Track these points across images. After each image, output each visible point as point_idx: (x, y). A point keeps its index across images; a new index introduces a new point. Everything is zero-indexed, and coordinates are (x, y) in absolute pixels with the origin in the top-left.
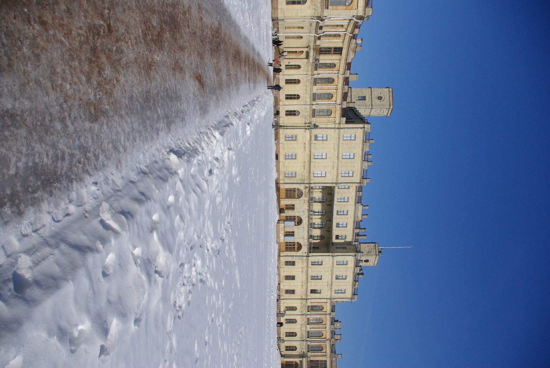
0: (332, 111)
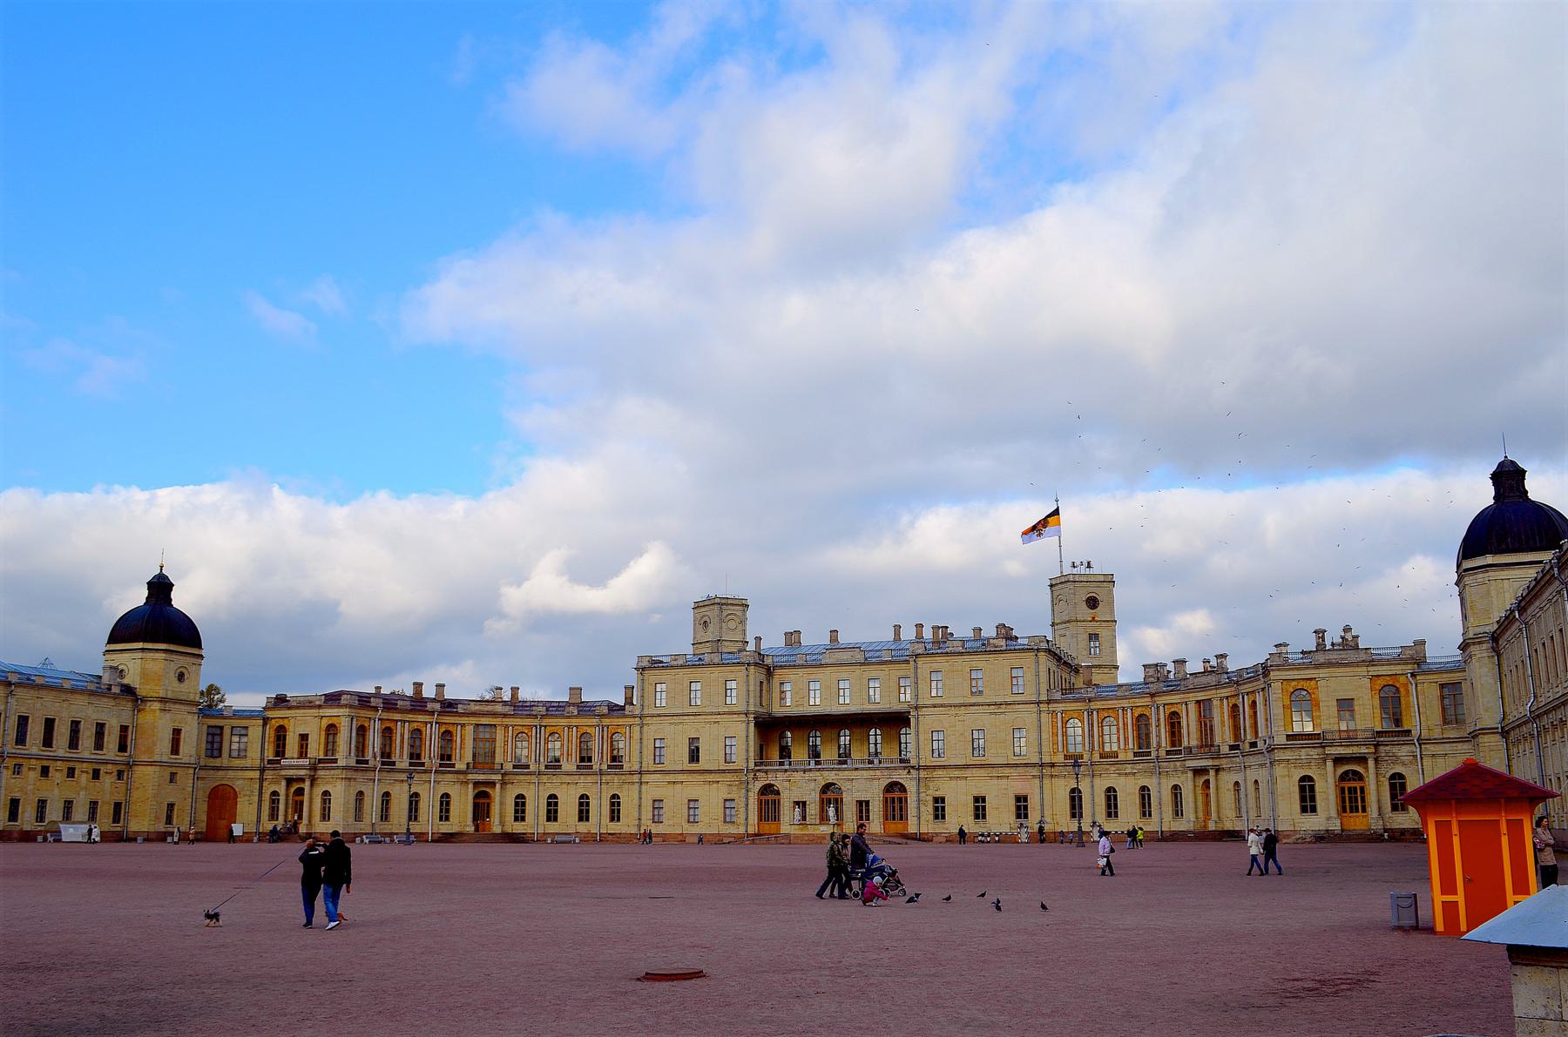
0: (613, 732)
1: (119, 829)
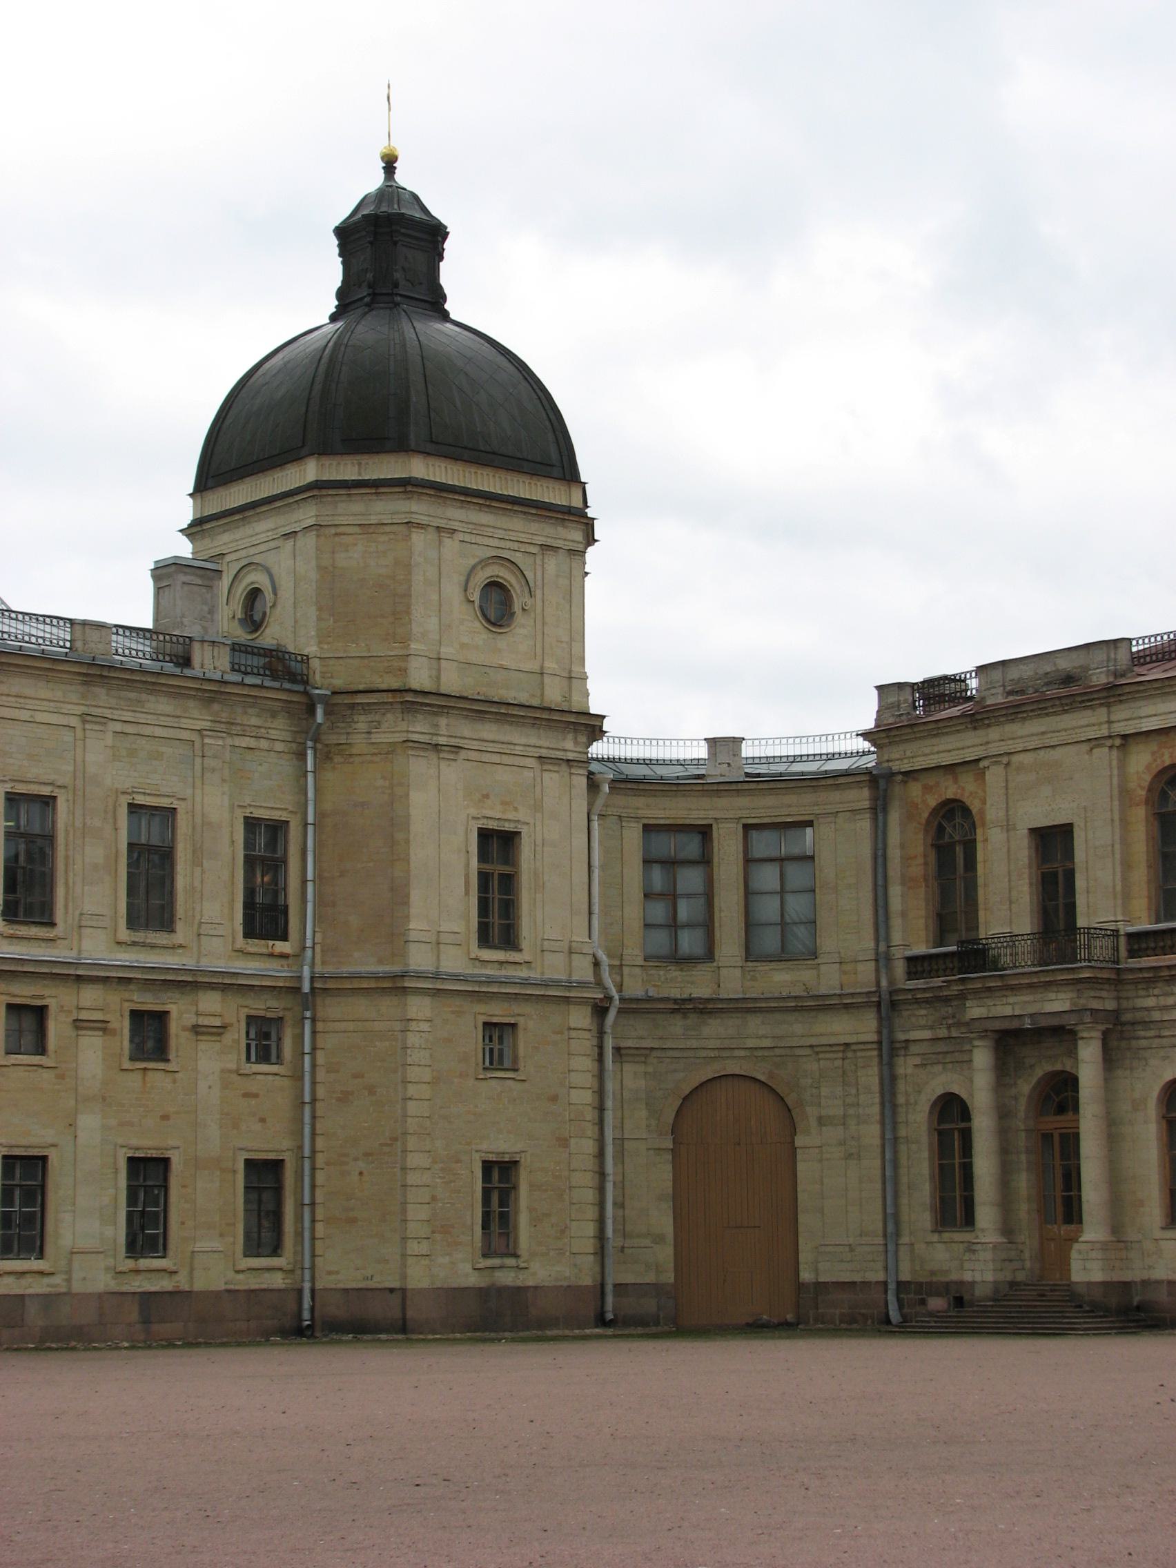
1: (277, 1281)
